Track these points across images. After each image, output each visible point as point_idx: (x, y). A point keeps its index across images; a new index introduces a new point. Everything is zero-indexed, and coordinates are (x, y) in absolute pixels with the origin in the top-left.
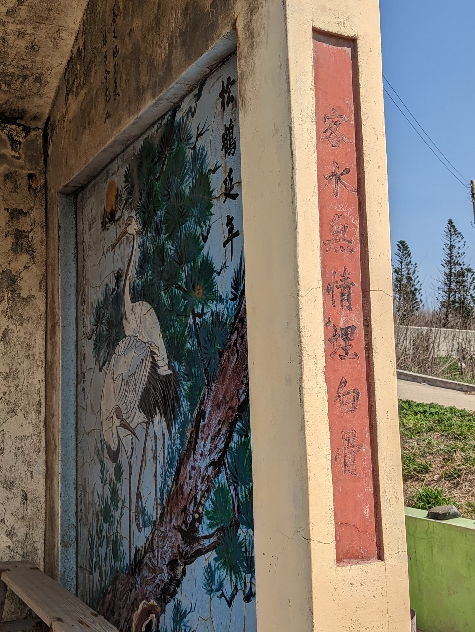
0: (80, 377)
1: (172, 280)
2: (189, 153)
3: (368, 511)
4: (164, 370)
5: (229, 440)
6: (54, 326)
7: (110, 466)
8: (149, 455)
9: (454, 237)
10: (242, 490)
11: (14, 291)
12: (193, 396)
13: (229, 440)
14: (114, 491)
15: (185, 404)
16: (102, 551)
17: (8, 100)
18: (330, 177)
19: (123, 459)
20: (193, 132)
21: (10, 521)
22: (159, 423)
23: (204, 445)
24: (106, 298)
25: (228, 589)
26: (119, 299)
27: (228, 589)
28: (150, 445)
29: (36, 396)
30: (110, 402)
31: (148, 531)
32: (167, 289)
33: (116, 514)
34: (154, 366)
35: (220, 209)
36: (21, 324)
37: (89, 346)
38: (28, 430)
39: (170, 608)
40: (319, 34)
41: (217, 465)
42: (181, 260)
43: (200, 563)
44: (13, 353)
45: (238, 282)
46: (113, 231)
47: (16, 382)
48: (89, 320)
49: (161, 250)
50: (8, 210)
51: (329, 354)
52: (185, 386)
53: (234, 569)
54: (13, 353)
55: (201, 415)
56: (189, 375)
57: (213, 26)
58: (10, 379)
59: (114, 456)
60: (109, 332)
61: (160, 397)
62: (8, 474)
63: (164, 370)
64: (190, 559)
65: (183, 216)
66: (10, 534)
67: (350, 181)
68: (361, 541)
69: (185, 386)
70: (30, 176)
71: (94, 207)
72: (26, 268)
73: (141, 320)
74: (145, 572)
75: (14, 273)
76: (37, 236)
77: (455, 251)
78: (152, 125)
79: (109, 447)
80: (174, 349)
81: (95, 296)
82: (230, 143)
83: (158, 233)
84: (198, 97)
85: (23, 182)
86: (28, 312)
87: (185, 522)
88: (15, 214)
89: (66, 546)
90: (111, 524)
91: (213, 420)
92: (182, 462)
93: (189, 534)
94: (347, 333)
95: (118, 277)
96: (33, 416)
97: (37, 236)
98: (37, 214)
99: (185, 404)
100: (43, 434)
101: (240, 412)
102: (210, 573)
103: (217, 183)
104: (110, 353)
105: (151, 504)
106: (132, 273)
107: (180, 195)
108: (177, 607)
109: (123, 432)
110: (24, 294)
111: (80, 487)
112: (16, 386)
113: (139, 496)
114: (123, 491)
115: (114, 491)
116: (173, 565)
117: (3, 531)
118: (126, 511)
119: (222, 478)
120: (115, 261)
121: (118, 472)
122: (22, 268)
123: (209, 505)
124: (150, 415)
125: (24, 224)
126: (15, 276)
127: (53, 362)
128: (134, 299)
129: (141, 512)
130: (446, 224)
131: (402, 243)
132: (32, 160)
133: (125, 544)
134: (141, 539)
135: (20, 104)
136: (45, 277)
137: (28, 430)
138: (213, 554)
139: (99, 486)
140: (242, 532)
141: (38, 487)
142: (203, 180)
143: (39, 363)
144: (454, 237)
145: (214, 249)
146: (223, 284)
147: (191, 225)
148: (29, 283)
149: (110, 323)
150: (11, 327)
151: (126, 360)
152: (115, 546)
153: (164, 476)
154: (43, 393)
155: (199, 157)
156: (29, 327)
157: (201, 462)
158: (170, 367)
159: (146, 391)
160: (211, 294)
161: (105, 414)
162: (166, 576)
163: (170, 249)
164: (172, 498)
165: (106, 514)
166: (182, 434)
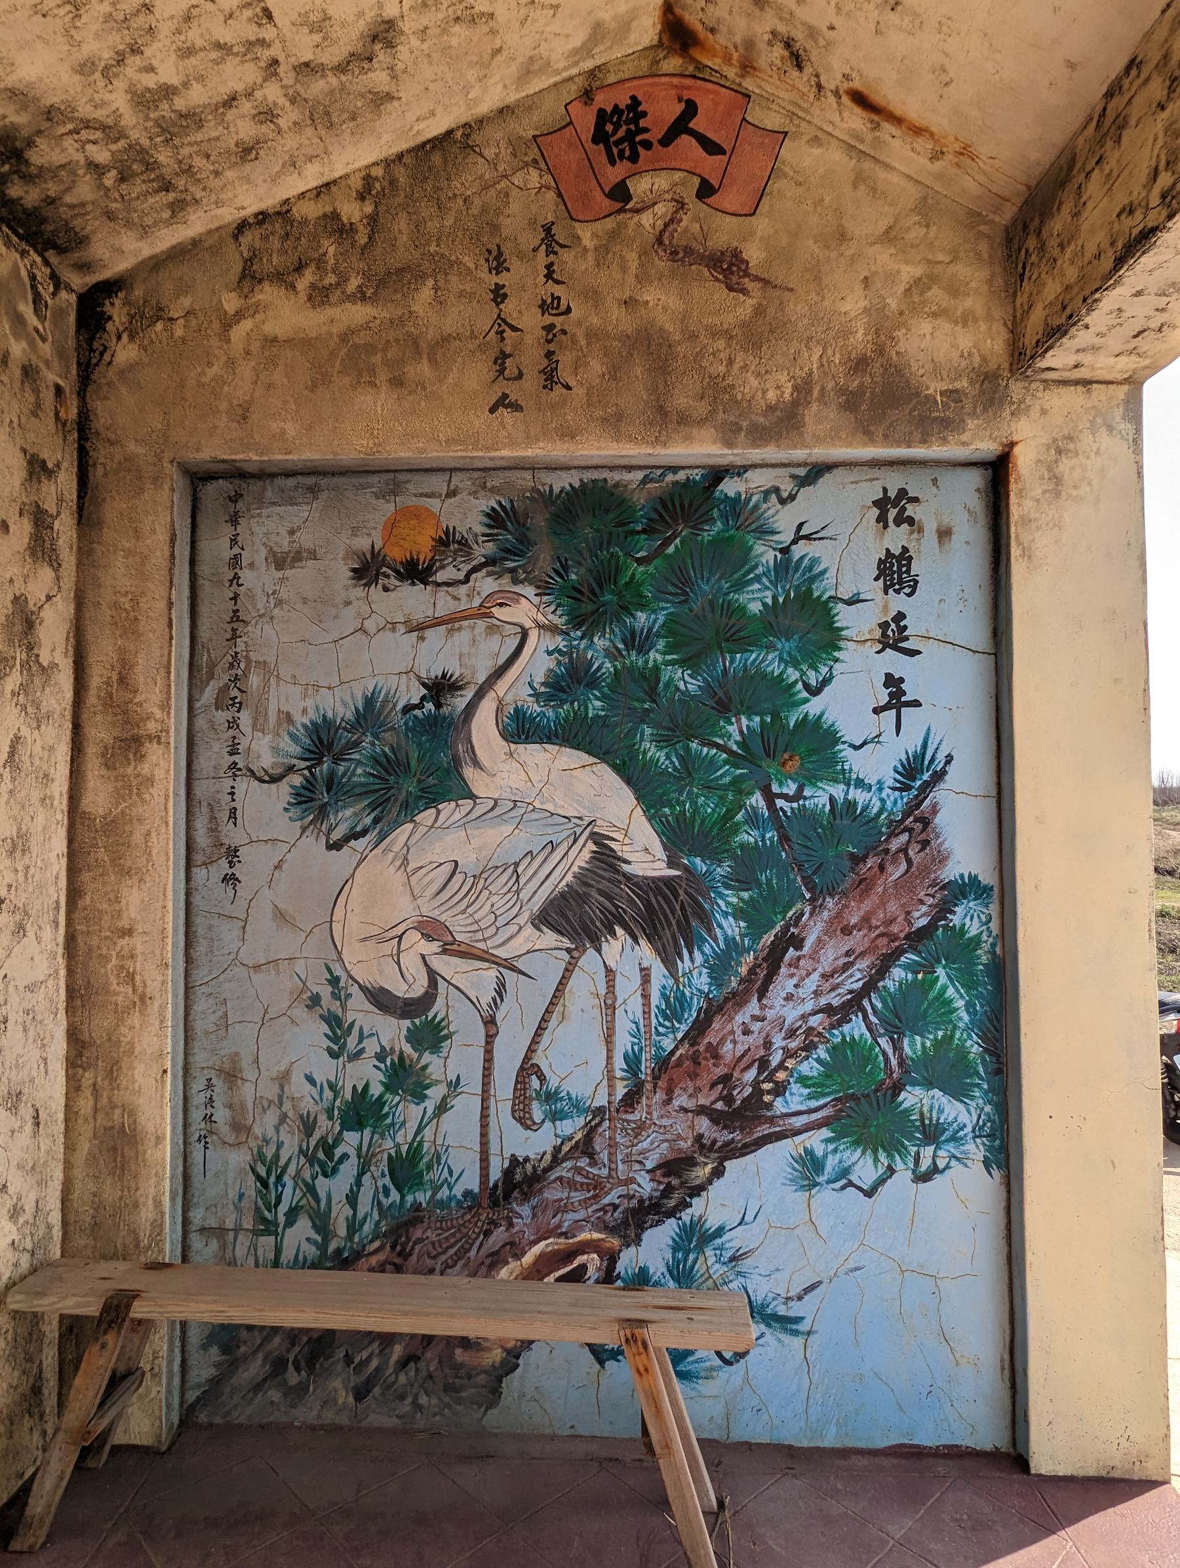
11: (30, 648)
17: (83, 205)
21: (17, 1183)
29: (52, 891)
36: (39, 727)
44: (24, 793)
47: (26, 860)
50: (24, 451)
54: (24, 793)
58: (18, 853)
62: (13, 1076)
72: (49, 598)
75: (31, 603)
78: (640, 468)
80: (678, 837)
87: (729, 1099)
96: (47, 933)
97: (65, 529)
100: (63, 973)
110: (45, 660)
111: (207, 1080)
112: (27, 868)
117: (5, 1211)
122: (43, 599)
123: (811, 1068)
126: (33, 613)
135: (92, 224)
138: (826, 1133)
143: (59, 817)
150: (25, 732)
154: (63, 883)
158: (671, 864)
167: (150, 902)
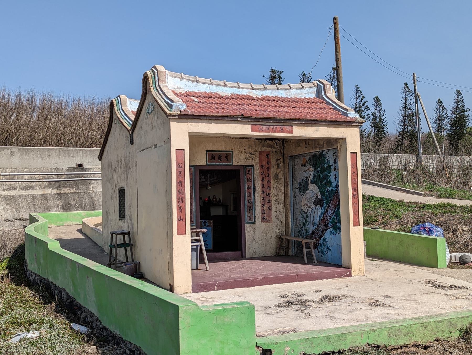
0: (294, 196)
1: (322, 182)
2: (326, 161)
3: (358, 220)
4: (320, 197)
5: (335, 210)
6: (287, 185)
7: (305, 215)
8: (316, 213)
9: (408, 93)
10: (338, 218)
12: (327, 203)
13: (335, 210)
14: (306, 220)
15: (325, 204)
16: (302, 232)
18: (353, 173)
19: (309, 214)
20: (327, 157)
21: (279, 227)
22: (319, 207)
23: (329, 211)
24: (302, 181)
25: (335, 233)
26: (307, 182)
27: (335, 233)
28: (316, 211)
30: (304, 202)
31: (316, 226)
32: (320, 183)
33: (307, 224)
34: (317, 196)
35: (333, 173)
37: (297, 191)
38: (281, 208)
39: (322, 239)
40: (351, 153)
41: (332, 214)
42: (324, 179)
43: (329, 230)
45: (337, 185)
46: (305, 168)
48: (297, 185)
49: (319, 176)
51: (353, 198)
52: (325, 201)
53: (336, 230)
55: (329, 206)
56: (326, 199)
57: (333, 145)
59: (306, 213)
60: (304, 188)
61: (318, 202)
63: (320, 197)
64: (326, 230)
65: (325, 171)
66: (279, 229)
67: (355, 173)
68: (357, 224)
69: (325, 201)
70: (280, 151)
71: (298, 161)
73: (313, 188)
74: (315, 234)
76: (282, 165)
77: (408, 101)
79: (304, 212)
80: (322, 194)
81: (299, 180)
82: (335, 162)
83: (318, 172)
84: (328, 151)
85: (279, 153)
86: (281, 182)
88: (277, 160)
89: (292, 232)
90: (305, 226)
91: (332, 207)
92: (324, 214)
93: (326, 226)
94: (355, 195)
95: (307, 178)
97: (282, 165)
98: (282, 160)
99: (325, 204)
101: (338, 206)
102: (331, 231)
103: (332, 168)
104: (304, 193)
105: (317, 222)
106: (311, 178)
107: (324, 167)
108: (324, 238)
109: (308, 208)
111: (295, 220)
113: (313, 220)
114: (309, 219)
115: (306, 220)
116: (322, 231)
118: (310, 224)
119: (334, 216)
120: (306, 174)
121: (307, 216)
123: (331, 221)
124: (316, 205)
125: (279, 162)
127: (287, 193)
128: (311, 183)
129: (314, 223)
130: (403, 85)
131: (377, 97)
132: (280, 147)
133: (310, 230)
134: (314, 228)
136: (284, 174)
137: (281, 208)
139: (301, 219)
140: (338, 224)
141: (284, 220)
142: (329, 166)
144: (408, 93)
145: (332, 178)
146: (334, 185)
147: (326, 173)
148: (281, 175)
149: (304, 186)
151: (308, 195)
152: (307, 231)
153: (320, 216)
155: (328, 162)
156: (281, 185)
157: (329, 213)
159: (315, 201)
160: (331, 185)
161: (303, 205)
162: (321, 234)
163: (321, 176)
164: (321, 221)
165: (304, 224)
166: (324, 209)
167: (289, 202)
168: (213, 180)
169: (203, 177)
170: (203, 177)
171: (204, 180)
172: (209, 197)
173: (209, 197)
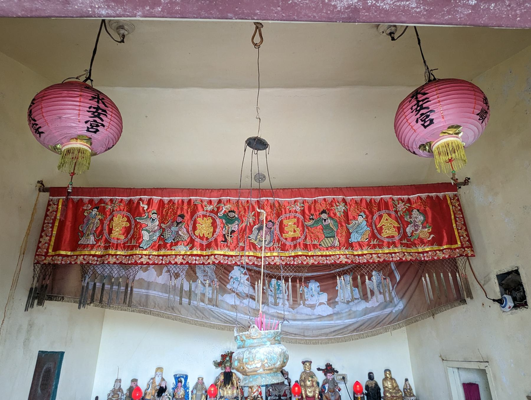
168: (366, 311)
169: (324, 297)
170: (324, 297)
171: (329, 310)
172: (371, 376)
173: (371, 376)
